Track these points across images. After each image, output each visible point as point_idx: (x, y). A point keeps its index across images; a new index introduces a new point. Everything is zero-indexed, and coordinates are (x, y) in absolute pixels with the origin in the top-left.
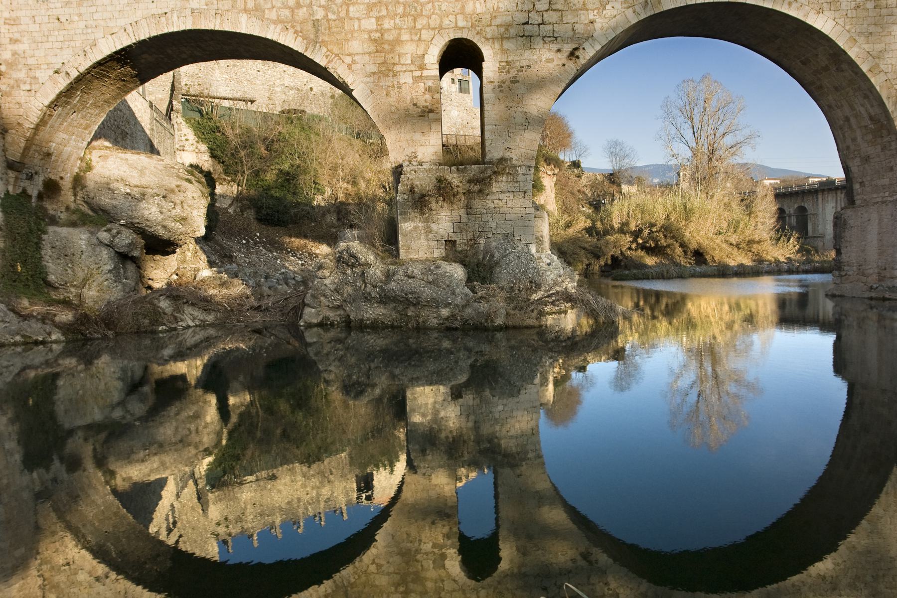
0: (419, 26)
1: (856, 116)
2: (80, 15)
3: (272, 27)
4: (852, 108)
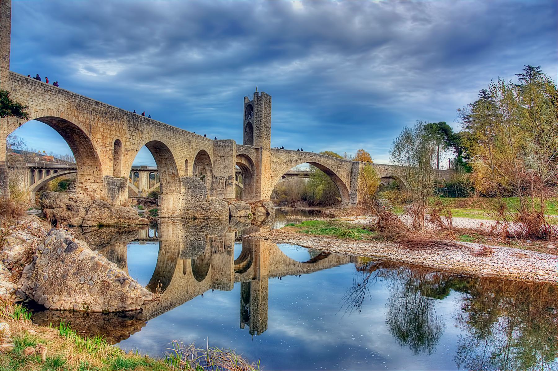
1: (168, 171)
2: (26, 100)
3: (81, 123)
4: (168, 169)
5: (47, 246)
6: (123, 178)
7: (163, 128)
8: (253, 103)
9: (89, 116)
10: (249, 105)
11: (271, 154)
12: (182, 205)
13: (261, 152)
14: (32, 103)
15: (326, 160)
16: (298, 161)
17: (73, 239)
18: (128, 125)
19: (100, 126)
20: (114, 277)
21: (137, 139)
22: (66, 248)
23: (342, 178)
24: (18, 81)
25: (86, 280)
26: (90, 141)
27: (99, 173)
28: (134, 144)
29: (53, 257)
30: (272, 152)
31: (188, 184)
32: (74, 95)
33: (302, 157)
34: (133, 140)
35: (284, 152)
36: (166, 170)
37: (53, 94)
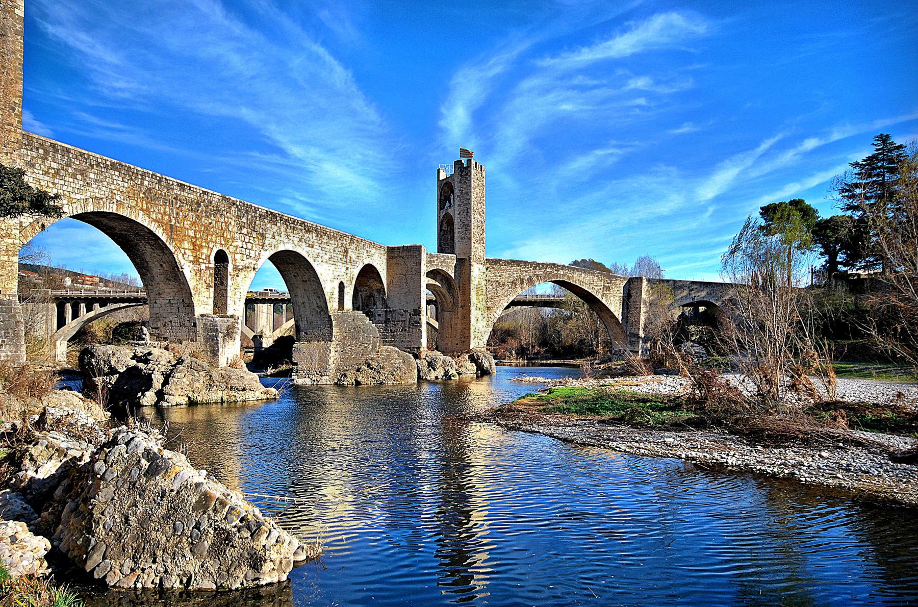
0: (209, 240)
2: (54, 183)
3: (153, 223)
5: (112, 465)
6: (232, 317)
7: (300, 227)
8: (453, 180)
9: (167, 209)
10: (446, 183)
11: (487, 269)
12: (335, 362)
13: (470, 265)
14: (65, 188)
15: (583, 275)
16: (534, 278)
17: (159, 449)
18: (237, 224)
19: (187, 227)
20: (238, 521)
21: (254, 248)
22: (147, 467)
23: (613, 307)
24: (37, 149)
25: (185, 527)
26: (171, 253)
27: (188, 310)
28: (249, 257)
29: (122, 486)
30: (488, 265)
31: (346, 325)
32: (140, 173)
33: (541, 273)
34: (248, 251)
35: (509, 264)
36: (306, 300)
37: (102, 172)
